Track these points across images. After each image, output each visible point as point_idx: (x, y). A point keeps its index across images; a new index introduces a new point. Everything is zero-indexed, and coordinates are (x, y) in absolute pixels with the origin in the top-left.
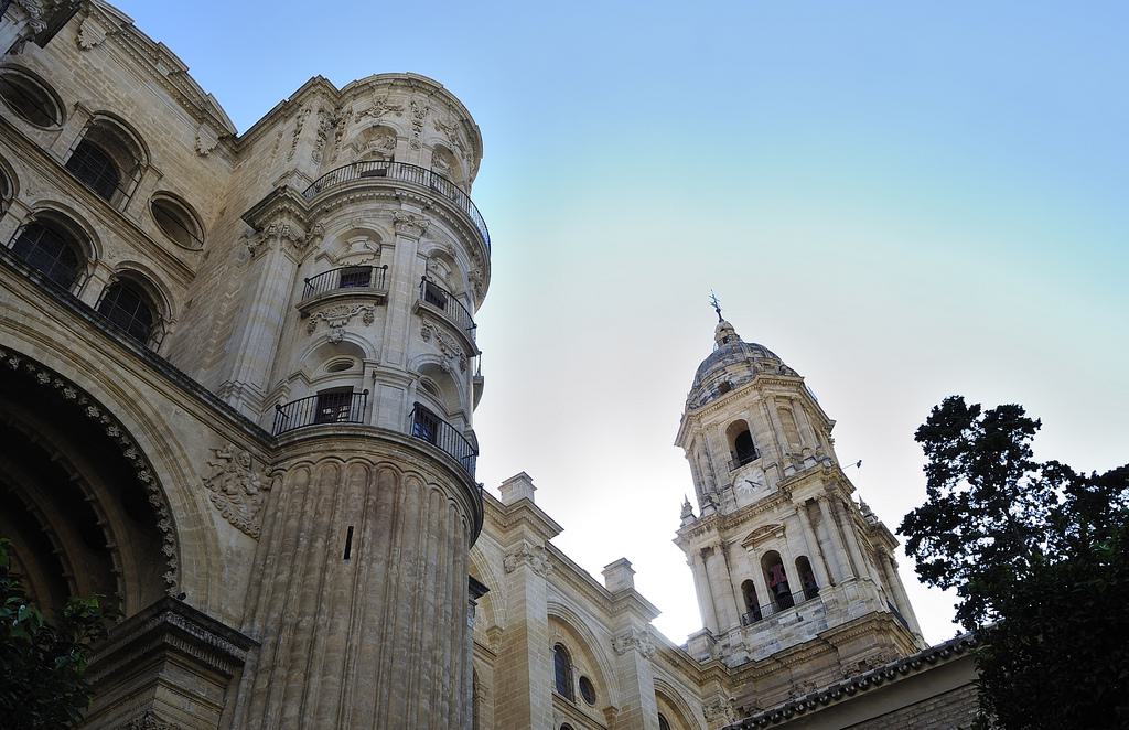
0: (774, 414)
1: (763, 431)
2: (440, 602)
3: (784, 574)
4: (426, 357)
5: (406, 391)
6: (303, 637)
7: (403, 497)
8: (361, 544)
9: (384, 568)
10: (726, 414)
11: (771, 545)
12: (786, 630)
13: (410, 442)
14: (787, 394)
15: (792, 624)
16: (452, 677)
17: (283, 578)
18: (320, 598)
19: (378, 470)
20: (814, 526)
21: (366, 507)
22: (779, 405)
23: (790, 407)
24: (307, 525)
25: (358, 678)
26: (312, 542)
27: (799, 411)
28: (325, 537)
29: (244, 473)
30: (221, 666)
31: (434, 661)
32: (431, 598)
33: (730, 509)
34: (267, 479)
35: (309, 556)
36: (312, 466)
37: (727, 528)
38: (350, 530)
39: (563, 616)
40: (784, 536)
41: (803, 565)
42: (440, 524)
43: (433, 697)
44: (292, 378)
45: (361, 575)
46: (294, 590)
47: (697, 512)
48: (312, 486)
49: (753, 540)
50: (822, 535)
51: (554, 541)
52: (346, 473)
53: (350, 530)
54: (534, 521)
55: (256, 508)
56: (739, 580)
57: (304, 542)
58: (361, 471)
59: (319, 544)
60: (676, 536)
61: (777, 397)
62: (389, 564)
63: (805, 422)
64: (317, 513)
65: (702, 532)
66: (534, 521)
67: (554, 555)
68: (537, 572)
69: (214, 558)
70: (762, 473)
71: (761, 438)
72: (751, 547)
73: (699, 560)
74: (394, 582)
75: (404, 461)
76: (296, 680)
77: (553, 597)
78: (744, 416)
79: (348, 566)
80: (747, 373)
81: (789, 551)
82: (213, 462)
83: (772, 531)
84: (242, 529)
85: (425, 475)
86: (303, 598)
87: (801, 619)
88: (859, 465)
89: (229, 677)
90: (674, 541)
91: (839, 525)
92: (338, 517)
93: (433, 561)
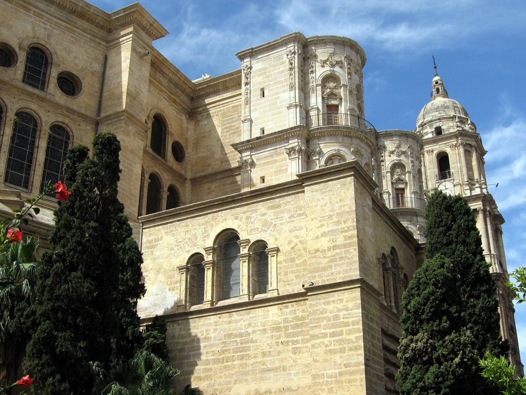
14: (470, 142)
22: (466, 148)
23: (470, 149)
70: (452, 186)
78: (448, 150)
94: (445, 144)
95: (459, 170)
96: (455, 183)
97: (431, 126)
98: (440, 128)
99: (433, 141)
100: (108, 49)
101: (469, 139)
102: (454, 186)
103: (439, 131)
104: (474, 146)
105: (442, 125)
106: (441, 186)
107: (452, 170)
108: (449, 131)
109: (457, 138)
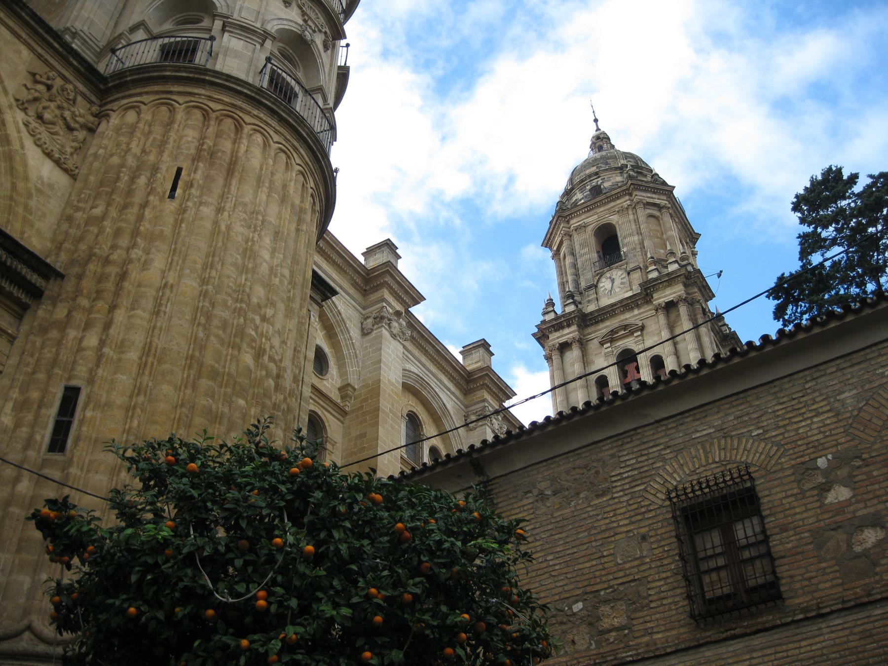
0: (642, 219)
1: (631, 235)
2: (276, 262)
3: (638, 372)
4: (285, 22)
5: (258, 46)
6: (113, 271)
7: (243, 148)
8: (190, 185)
9: (213, 214)
10: (596, 217)
11: (630, 343)
13: (256, 93)
14: (658, 202)
16: (284, 342)
17: (97, 211)
18: (135, 233)
19: (217, 118)
21: (199, 150)
23: (657, 213)
24: (131, 161)
25: (170, 318)
26: (133, 179)
27: (667, 219)
28: (148, 174)
29: (65, 105)
30: (16, 292)
31: (264, 319)
32: (266, 255)
33: (591, 308)
34: (91, 119)
35: (130, 193)
36: (143, 107)
37: (587, 326)
38: (179, 171)
39: (417, 386)
40: (642, 335)
42: (285, 187)
43: (259, 354)
44: (134, 29)
45: (186, 216)
46: (107, 223)
47: (559, 309)
48: (141, 125)
49: (611, 337)
51: (414, 310)
52: (180, 115)
53: (179, 171)
54: (395, 287)
55: (75, 144)
57: (125, 178)
58: (198, 114)
59: (142, 180)
60: (536, 330)
61: (648, 204)
62: (219, 210)
63: (673, 231)
64: (143, 151)
65: (563, 328)
66: (395, 287)
67: (414, 324)
68: (394, 336)
69: (21, 185)
70: (625, 275)
71: (628, 241)
72: (609, 345)
73: (556, 357)
74: (223, 228)
75: (248, 113)
76: (99, 312)
77: (408, 366)
78: (614, 219)
79: (171, 206)
82: (29, 85)
83: (629, 330)
84: (57, 162)
85: (272, 133)
86: (118, 233)
88: (719, 275)
89: (25, 308)
90: (534, 335)
92: (166, 157)
93: (272, 219)
94: (608, 209)
95: (638, 247)
96: (628, 269)
98: (600, 186)
99: (589, 208)
101: (654, 196)
102: (629, 274)
103: (597, 191)
104: (664, 207)
105: (603, 182)
106: (603, 280)
107: (624, 250)
109: (631, 195)
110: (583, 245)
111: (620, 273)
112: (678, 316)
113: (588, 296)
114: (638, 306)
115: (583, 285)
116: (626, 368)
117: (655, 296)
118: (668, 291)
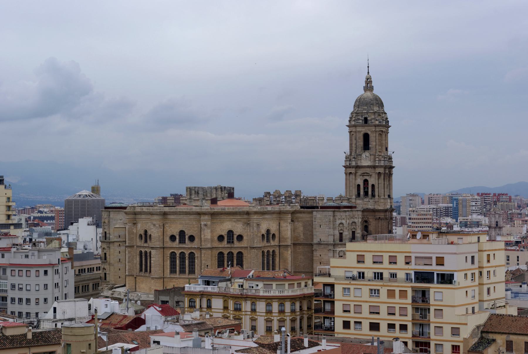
11: (367, 178)
12: (365, 203)
14: (382, 130)
15: (367, 202)
20: (378, 179)
23: (381, 133)
40: (371, 177)
41: (373, 186)
49: (363, 175)
50: (380, 182)
56: (357, 184)
70: (369, 155)
71: (372, 144)
73: (348, 175)
78: (369, 133)
80: (373, 117)
81: (372, 181)
87: (369, 201)
91: (384, 181)
97: (362, 116)
100: (280, 220)
101: (382, 127)
102: (370, 155)
103: (366, 120)
108: (371, 121)
110: (359, 138)
111: (368, 154)
112: (381, 176)
113: (359, 158)
114: (371, 168)
115: (357, 152)
116: (365, 183)
117: (376, 169)
118: (380, 169)
